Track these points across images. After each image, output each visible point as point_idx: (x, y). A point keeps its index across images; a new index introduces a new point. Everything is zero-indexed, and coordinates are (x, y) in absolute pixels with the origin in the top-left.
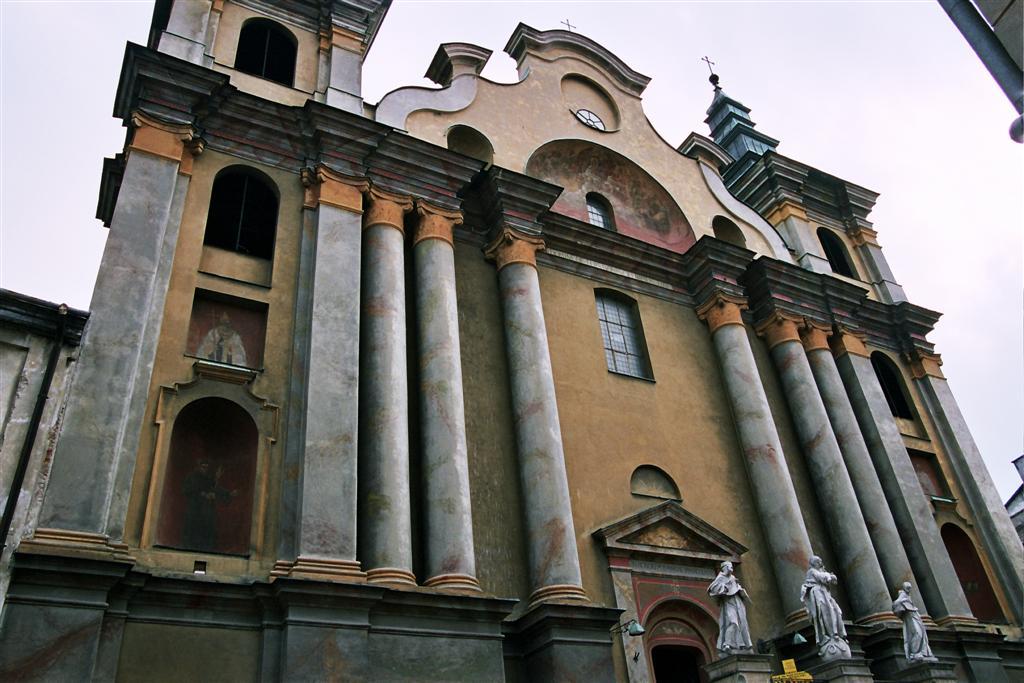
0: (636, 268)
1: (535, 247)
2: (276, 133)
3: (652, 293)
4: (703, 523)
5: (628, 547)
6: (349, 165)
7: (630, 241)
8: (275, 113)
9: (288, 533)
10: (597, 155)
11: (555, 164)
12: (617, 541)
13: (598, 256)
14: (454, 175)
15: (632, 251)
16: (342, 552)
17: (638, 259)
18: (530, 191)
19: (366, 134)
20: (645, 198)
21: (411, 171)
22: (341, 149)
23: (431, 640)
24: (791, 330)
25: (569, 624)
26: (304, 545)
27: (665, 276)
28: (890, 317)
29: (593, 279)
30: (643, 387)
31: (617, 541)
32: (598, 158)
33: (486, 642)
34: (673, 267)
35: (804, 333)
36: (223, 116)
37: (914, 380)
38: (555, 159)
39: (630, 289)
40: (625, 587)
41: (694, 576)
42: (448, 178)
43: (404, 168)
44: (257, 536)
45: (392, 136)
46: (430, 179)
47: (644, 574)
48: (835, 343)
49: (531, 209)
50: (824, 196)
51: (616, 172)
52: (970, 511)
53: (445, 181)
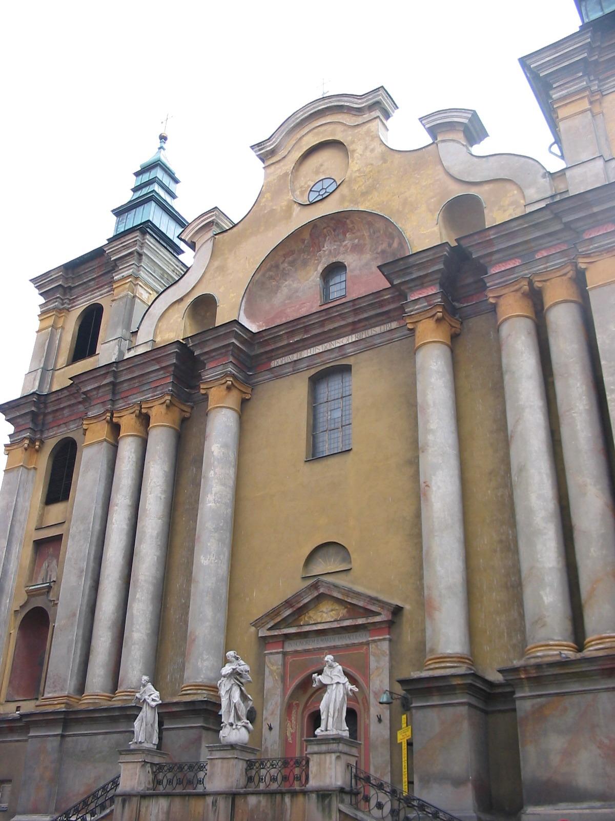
0: (354, 328)
1: (225, 386)
2: (73, 405)
3: (367, 346)
5: (276, 633)
6: (101, 405)
7: (335, 309)
8: (68, 394)
10: (325, 225)
11: (292, 264)
12: (269, 629)
13: (314, 340)
14: (164, 365)
15: (342, 316)
17: (350, 320)
18: (216, 339)
19: (105, 375)
20: (381, 232)
21: (141, 379)
22: (100, 395)
23: (94, 738)
29: (309, 367)
31: (269, 629)
32: (328, 226)
33: (123, 734)
34: (389, 303)
36: (49, 413)
38: (291, 259)
39: (345, 356)
40: (274, 668)
41: (348, 642)
42: (162, 368)
43: (137, 381)
45: (120, 365)
46: (153, 377)
47: (296, 652)
49: (223, 351)
51: (350, 226)
53: (162, 372)
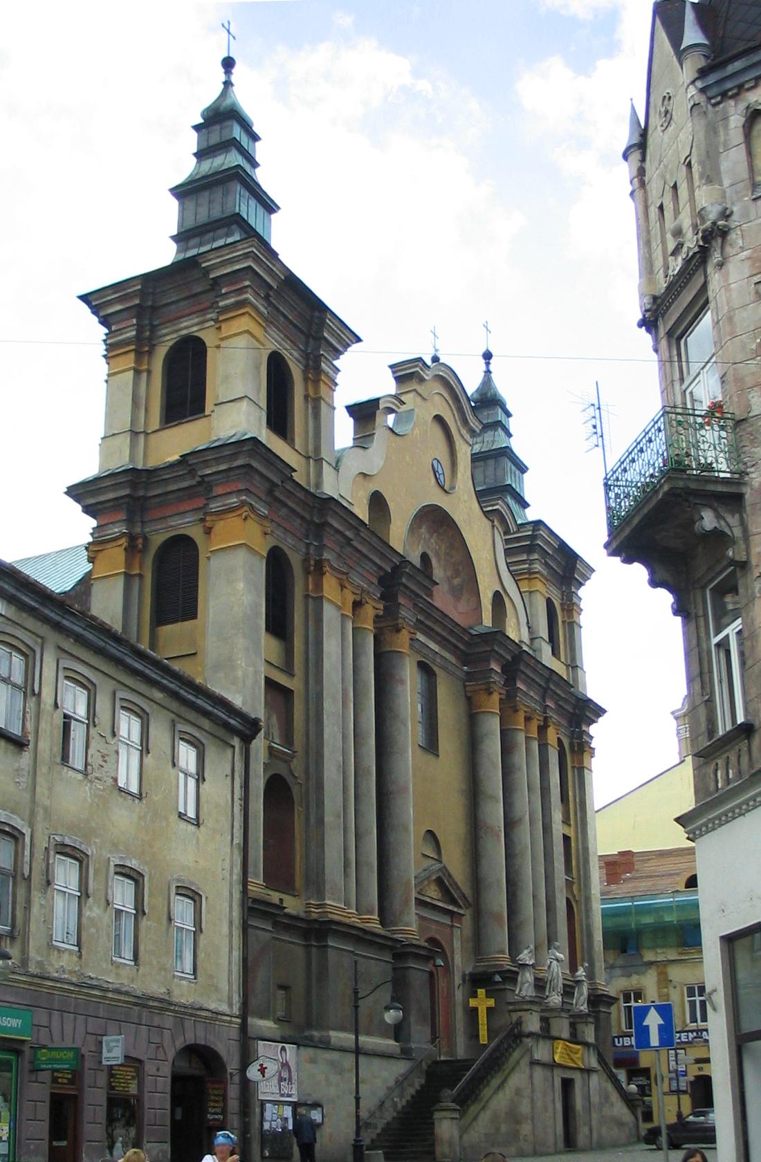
4: (456, 884)
9: (316, 883)
16: (339, 900)
24: (521, 716)
25: (417, 957)
26: (327, 895)
27: (454, 649)
28: (575, 707)
29: (418, 652)
30: (431, 757)
35: (528, 719)
37: (573, 767)
44: (299, 882)
48: (542, 729)
50: (558, 563)
52: (580, 890)
